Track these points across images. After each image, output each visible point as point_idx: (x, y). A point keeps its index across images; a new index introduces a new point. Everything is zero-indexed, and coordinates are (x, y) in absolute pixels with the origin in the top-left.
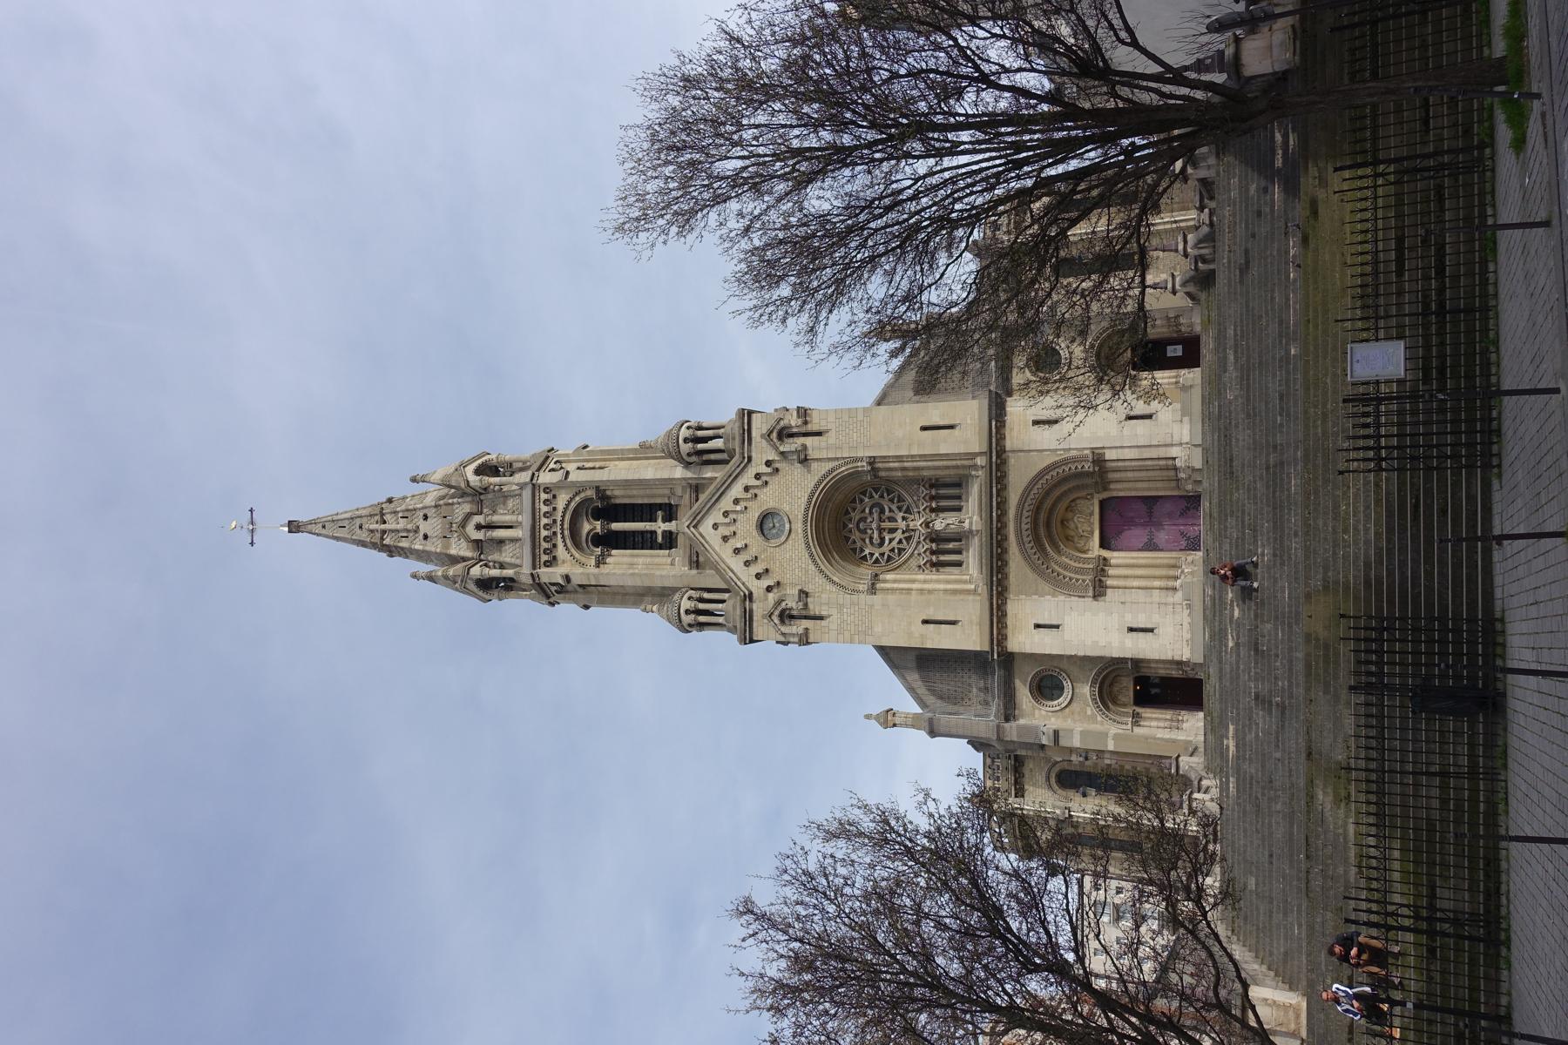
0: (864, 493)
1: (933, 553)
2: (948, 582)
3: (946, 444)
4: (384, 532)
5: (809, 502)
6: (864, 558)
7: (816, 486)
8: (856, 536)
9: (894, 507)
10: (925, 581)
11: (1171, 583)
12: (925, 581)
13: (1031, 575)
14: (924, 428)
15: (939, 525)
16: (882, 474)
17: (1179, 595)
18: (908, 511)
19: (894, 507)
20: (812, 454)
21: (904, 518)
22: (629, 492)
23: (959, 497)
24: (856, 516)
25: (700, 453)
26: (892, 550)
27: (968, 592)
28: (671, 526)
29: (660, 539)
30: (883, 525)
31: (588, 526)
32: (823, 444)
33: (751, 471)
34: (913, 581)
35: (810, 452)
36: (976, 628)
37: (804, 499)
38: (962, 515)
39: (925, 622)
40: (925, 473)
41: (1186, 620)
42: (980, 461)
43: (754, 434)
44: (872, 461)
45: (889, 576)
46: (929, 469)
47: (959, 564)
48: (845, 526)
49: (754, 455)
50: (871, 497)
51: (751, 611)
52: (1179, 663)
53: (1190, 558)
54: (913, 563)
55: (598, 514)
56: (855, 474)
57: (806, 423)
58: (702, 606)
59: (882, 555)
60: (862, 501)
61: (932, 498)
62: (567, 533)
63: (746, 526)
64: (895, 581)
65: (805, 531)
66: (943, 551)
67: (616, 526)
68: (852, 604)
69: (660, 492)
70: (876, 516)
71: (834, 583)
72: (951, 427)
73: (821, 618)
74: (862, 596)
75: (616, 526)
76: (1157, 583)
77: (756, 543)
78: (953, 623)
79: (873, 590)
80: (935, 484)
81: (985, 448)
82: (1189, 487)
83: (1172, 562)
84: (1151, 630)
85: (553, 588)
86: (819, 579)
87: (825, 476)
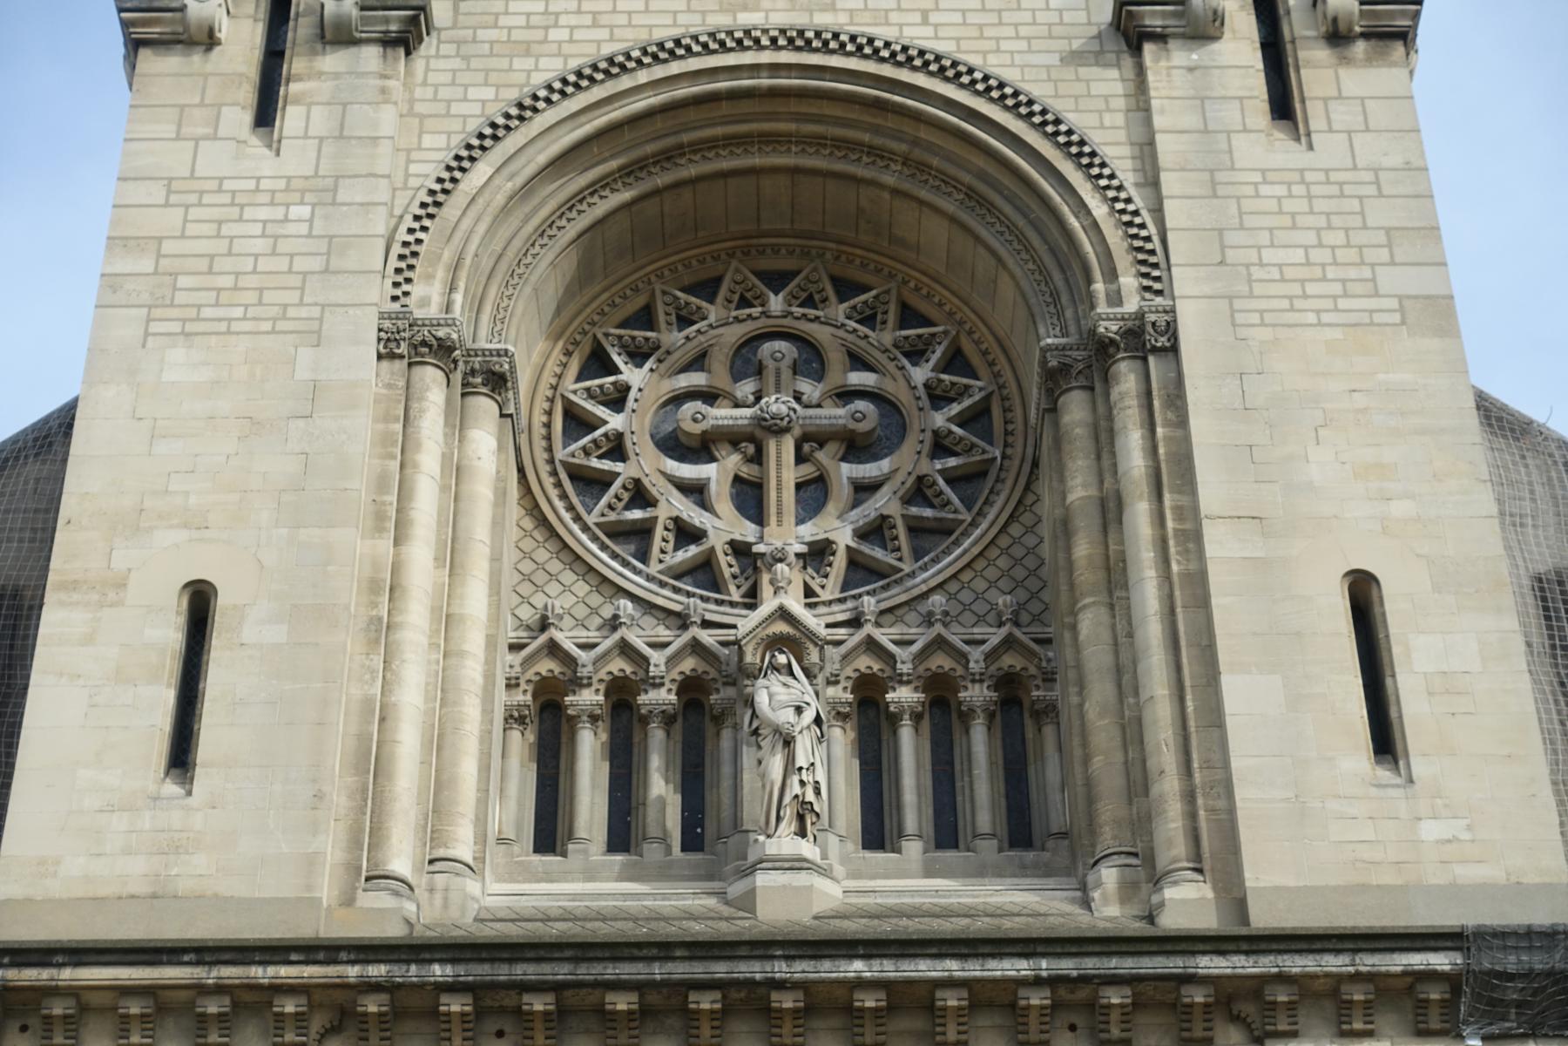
0: (955, 361)
1: (621, 696)
2: (439, 742)
3: (1281, 708)
5: (905, 57)
6: (598, 363)
7: (993, 88)
8: (721, 326)
9: (884, 503)
10: (447, 621)
12: (447, 621)
14: (1363, 595)
15: (779, 697)
16: (1075, 409)
18: (861, 571)
19: (884, 503)
20: (1168, 69)
21: (818, 554)
23: (947, 833)
24: (833, 324)
26: (640, 495)
27: (369, 828)
30: (781, 453)
32: (1229, 115)
34: (452, 557)
35: (1180, 56)
36: (130, 872)
37: (918, 36)
38: (839, 842)
39: (200, 605)
40: (1091, 622)
42: (1187, 903)
44: (1153, 341)
45: (485, 442)
46: (1115, 648)
47: (550, 833)
48: (776, 281)
50: (938, 397)
54: (568, 597)
56: (1064, 270)
57: (1337, 36)
59: (617, 448)
60: (916, 354)
61: (941, 700)
64: (456, 472)
66: (636, 736)
70: (835, 415)
71: (461, 163)
72: (1385, 740)
73: (265, 114)
74: (377, 292)
78: (181, 756)
79: (411, 345)
80: (1023, 706)
81: (1263, 918)
86: (483, 101)
87: (1049, 124)
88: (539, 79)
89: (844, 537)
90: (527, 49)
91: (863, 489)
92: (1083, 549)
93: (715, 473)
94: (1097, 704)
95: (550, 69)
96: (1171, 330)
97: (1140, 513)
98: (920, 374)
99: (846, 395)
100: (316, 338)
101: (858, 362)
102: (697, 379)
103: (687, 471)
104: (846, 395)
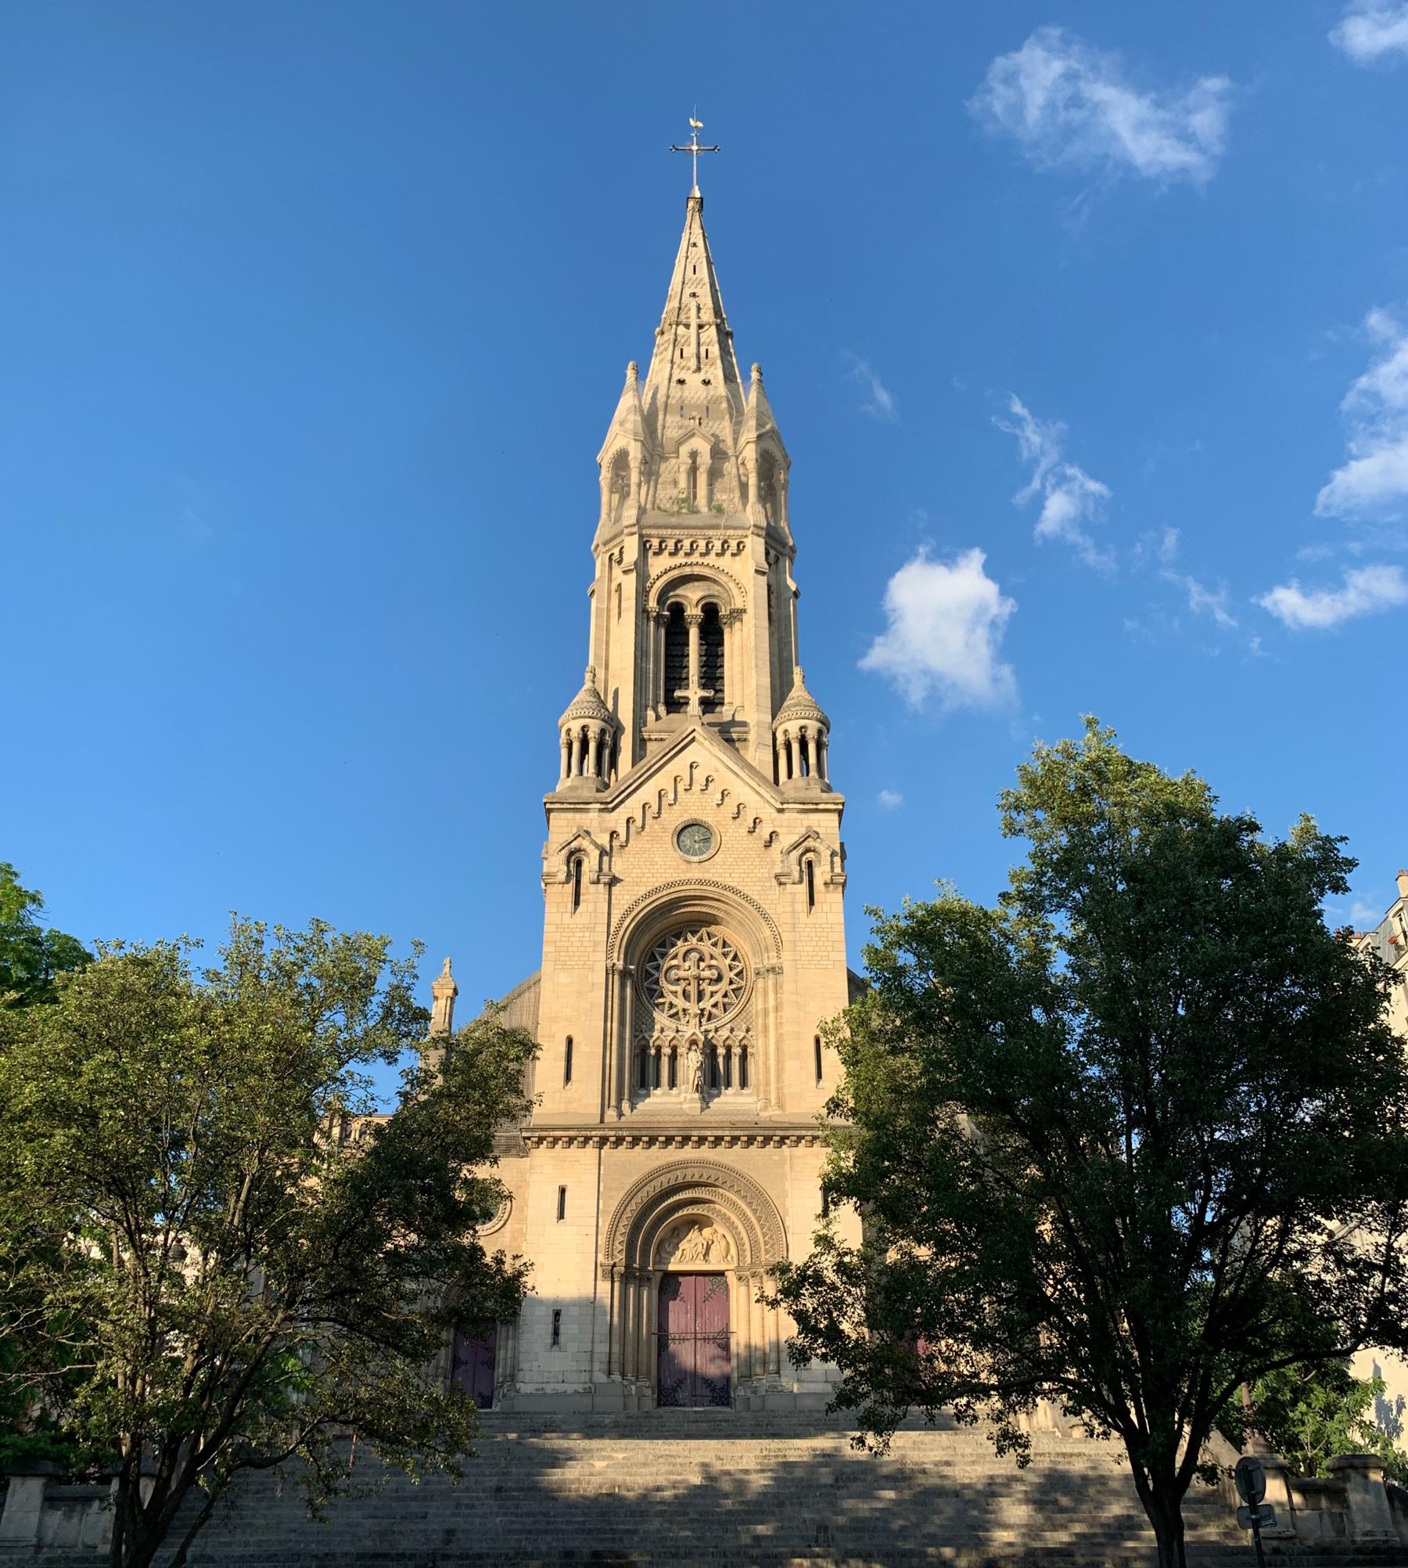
4: (687, 326)
5: (725, 888)
9: (718, 998)
11: (615, 1366)
13: (630, 1182)
17: (601, 1377)
19: (718, 998)
21: (702, 1010)
22: (736, 653)
25: (788, 746)
28: (694, 708)
29: (678, 693)
30: (694, 983)
31: (692, 598)
33: (767, 813)
37: (730, 882)
39: (570, 1041)
41: (570, 1388)
43: (814, 817)
49: (786, 815)
51: (587, 810)
52: (512, 1377)
53: (649, 1392)
55: (711, 611)
58: (592, 746)
60: (725, 955)
62: (687, 571)
63: (694, 806)
65: (689, 882)
67: (694, 634)
68: (596, 944)
69: (738, 693)
70: (707, 974)
73: (577, 903)
75: (694, 634)
76: (616, 1348)
77: (674, 818)
78: (568, 1077)
82: (741, 1392)
83: (643, 1369)
84: (555, 1342)
85: (616, 551)
88: (642, 893)
89: (709, 1008)
90: (637, 884)
91: (712, 994)
92: (760, 1021)
93: (679, 989)
94: (761, 1059)
95: (643, 891)
96: (781, 968)
97: (772, 1016)
98: (728, 961)
99: (710, 967)
100: (592, 969)
101: (712, 957)
102: (674, 962)
103: (673, 988)
104: (710, 967)
